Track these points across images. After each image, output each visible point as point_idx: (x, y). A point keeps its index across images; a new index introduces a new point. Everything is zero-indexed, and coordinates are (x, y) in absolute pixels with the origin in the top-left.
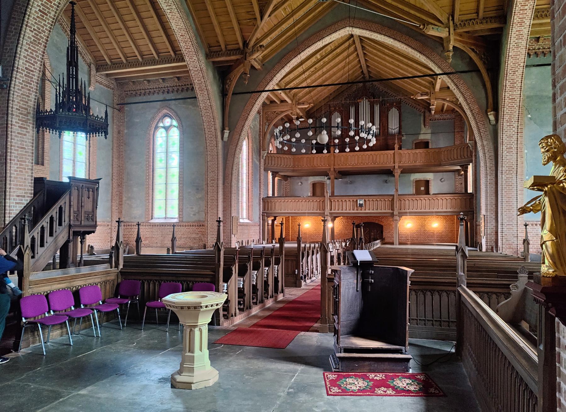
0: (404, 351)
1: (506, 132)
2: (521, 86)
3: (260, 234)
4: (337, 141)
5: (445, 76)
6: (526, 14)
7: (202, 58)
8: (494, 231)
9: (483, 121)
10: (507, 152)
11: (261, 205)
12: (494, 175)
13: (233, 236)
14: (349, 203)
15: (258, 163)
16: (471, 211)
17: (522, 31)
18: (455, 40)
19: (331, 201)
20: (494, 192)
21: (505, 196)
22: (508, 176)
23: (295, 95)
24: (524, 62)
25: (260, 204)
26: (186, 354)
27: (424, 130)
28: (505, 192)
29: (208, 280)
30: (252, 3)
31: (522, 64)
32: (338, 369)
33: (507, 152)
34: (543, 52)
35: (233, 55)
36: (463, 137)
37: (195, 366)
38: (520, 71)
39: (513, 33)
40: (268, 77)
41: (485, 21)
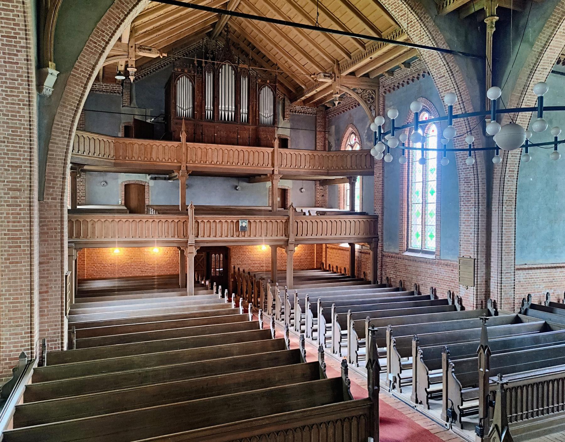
8: (484, 280)
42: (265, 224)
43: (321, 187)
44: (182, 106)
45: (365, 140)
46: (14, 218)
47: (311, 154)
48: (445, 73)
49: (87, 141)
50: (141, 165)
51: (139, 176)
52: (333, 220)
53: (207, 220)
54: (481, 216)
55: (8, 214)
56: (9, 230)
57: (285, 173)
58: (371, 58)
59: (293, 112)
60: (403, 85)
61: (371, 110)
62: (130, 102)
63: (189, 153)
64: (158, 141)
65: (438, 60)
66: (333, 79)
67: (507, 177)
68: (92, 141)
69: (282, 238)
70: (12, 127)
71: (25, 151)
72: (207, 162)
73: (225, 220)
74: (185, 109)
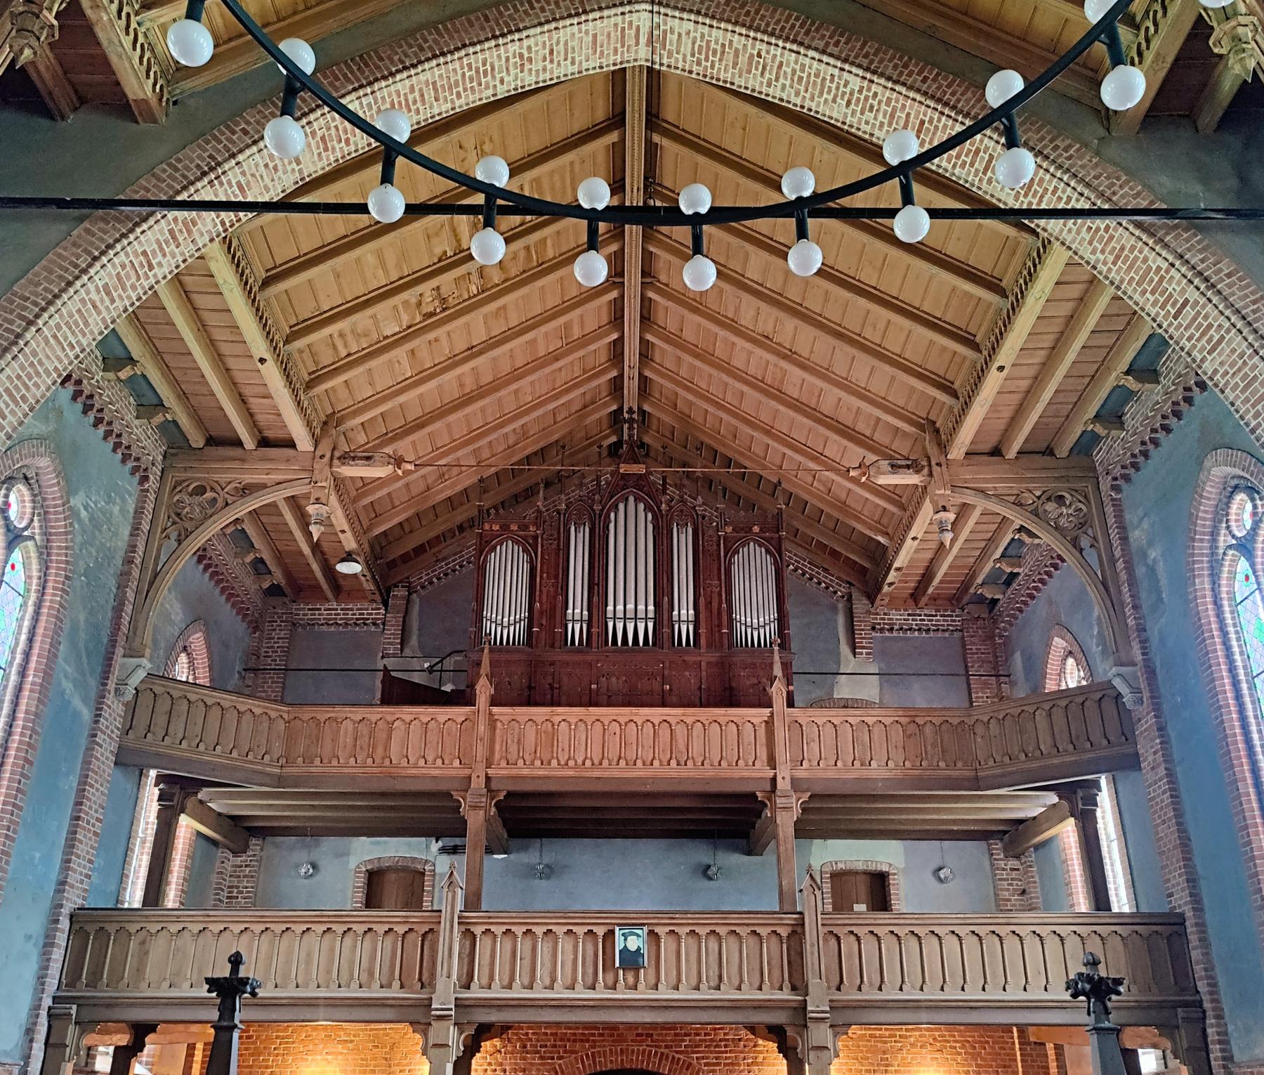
11: (58, 955)
14: (569, 947)
15: (86, 714)
16: (1186, 1004)
19: (469, 935)
25: (49, 944)
27: (849, 662)
42: (713, 945)
43: (1013, 863)
44: (499, 617)
45: (1098, 660)
47: (904, 720)
48: (1183, 291)
51: (409, 844)
52: (982, 931)
53: (504, 928)
57: (818, 789)
58: (1001, 368)
59: (882, 630)
60: (1155, 442)
61: (1081, 551)
62: (402, 644)
63: (498, 739)
65: (1145, 260)
68: (215, 713)
69: (779, 996)
72: (554, 762)
73: (565, 929)
74: (505, 624)
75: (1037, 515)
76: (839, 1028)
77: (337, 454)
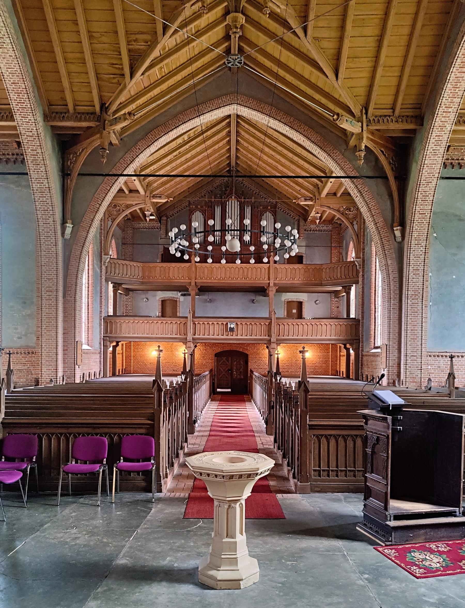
0: (458, 514)
1: (413, 251)
2: (433, 200)
3: (100, 364)
4: (210, 248)
5: (347, 179)
6: (449, 117)
7: (40, 118)
9: (388, 237)
10: (413, 274)
12: (398, 299)
13: (77, 367)
15: (99, 271)
17: (442, 136)
18: (368, 138)
19: (194, 324)
20: (397, 318)
21: (410, 323)
22: (413, 301)
23: (149, 185)
24: (439, 173)
25: (100, 325)
26: (224, 540)
28: (410, 319)
29: (142, 431)
30: (120, 52)
31: (437, 175)
32: (391, 541)
33: (413, 274)
34: (451, 163)
35: (85, 120)
36: (341, 254)
37: (238, 556)
38: (434, 183)
39: (432, 137)
40: (128, 157)
41: (401, 120)
42: (251, 326)
46: (49, 306)
49: (121, 266)
50: (161, 282)
51: (172, 293)
54: (393, 309)
55: (46, 304)
56: (46, 313)
57: (280, 286)
59: (308, 231)
61: (353, 225)
64: (173, 264)
66: (314, 201)
67: (412, 275)
68: (125, 267)
69: (265, 337)
70: (48, 258)
71: (54, 270)
72: (212, 278)
75: (343, 214)
76: (278, 344)
77: (152, 195)
